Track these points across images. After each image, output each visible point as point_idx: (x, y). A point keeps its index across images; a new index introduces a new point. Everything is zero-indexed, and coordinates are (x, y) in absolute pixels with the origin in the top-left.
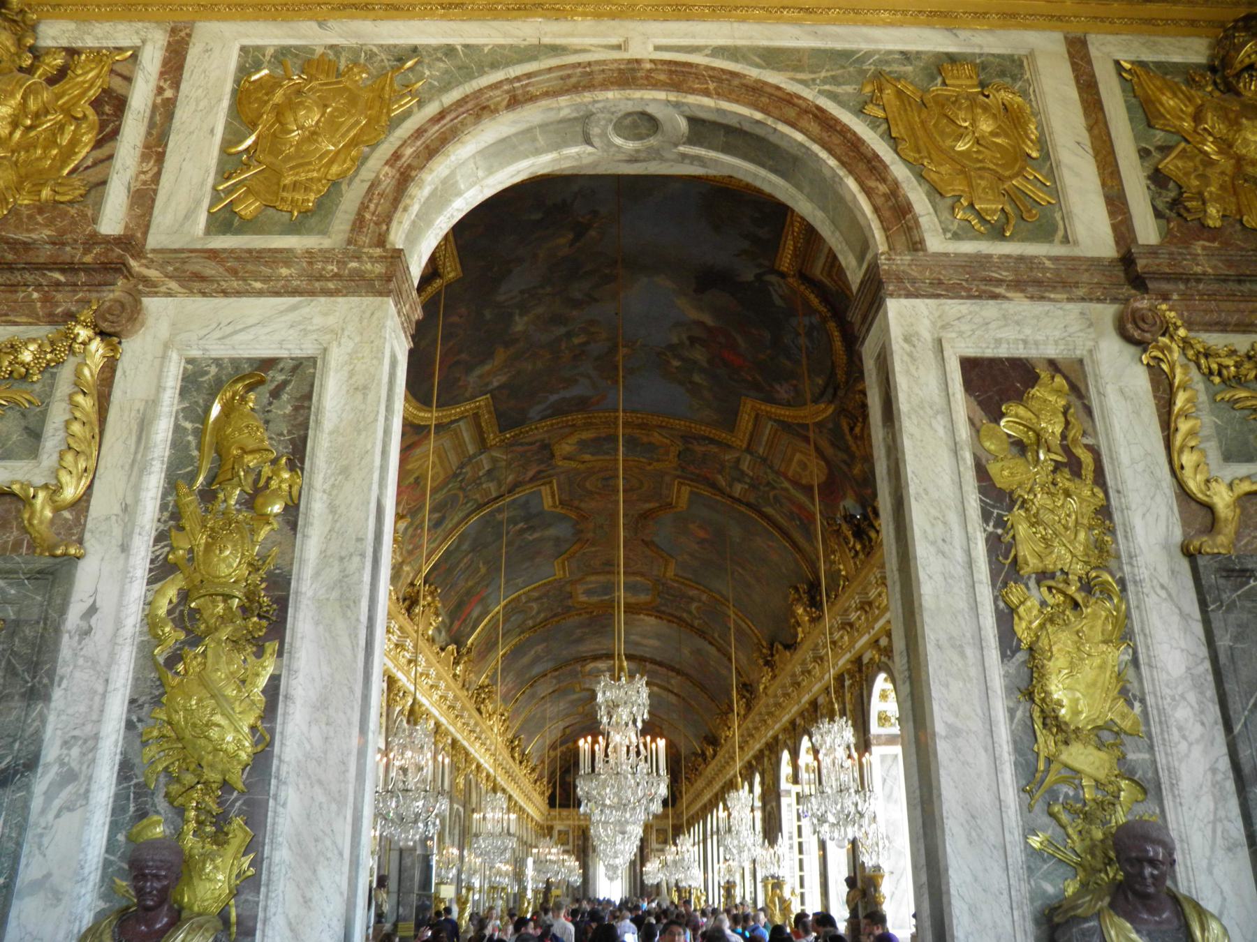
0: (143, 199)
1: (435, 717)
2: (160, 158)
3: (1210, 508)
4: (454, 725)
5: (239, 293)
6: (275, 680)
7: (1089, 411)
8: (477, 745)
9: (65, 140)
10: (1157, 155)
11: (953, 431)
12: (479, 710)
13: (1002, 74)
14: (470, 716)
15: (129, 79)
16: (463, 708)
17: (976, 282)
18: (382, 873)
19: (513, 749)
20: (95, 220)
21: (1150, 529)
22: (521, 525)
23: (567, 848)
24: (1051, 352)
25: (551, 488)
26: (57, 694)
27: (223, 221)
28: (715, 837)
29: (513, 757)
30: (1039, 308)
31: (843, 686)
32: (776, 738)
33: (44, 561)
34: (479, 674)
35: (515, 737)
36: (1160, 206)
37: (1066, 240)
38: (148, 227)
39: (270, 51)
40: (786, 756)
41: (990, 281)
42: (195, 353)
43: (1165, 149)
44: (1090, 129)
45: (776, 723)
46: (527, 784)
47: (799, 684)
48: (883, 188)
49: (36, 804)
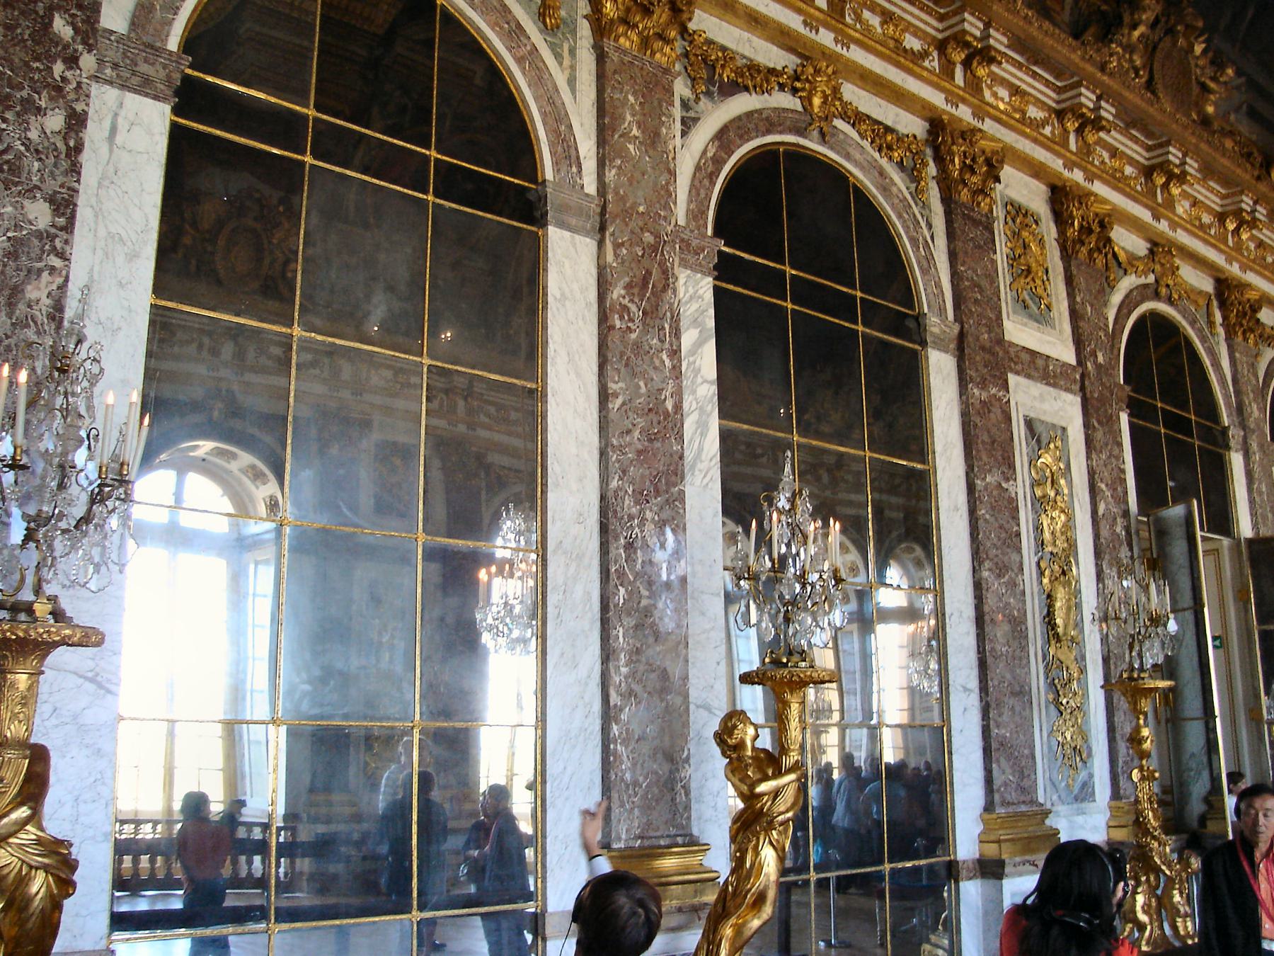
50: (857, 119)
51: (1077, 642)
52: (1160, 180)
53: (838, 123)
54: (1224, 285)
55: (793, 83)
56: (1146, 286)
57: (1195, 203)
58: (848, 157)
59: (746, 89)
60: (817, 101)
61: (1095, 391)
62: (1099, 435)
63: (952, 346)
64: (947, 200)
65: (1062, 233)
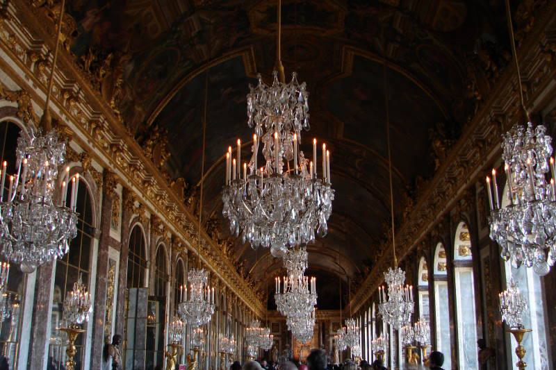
1: (171, 231)
4: (190, 241)
8: (210, 260)
12: (210, 236)
16: (196, 229)
18: (119, 333)
19: (239, 268)
22: (229, 89)
23: (277, 334)
25: (250, 54)
28: (370, 326)
31: (474, 195)
32: (415, 250)
35: (241, 260)
40: (422, 262)
45: (414, 239)
46: (250, 292)
47: (434, 205)
50: (92, 169)
51: (111, 324)
52: (146, 185)
53: (88, 171)
54: (153, 217)
55: (82, 157)
56: (136, 218)
57: (152, 191)
58: (87, 181)
59: (73, 160)
60: (86, 164)
61: (123, 251)
62: (123, 265)
63: (99, 237)
64: (104, 193)
65: (123, 202)
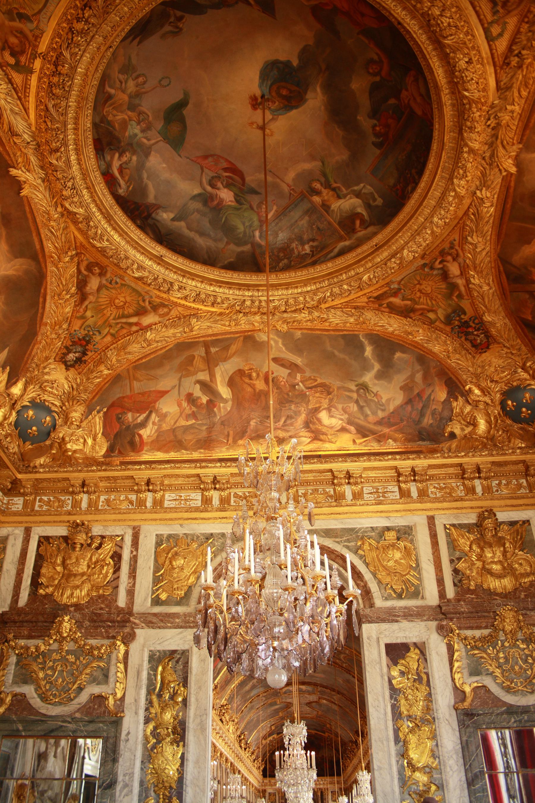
0: (131, 593)
2: (134, 577)
3: (464, 692)
5: (164, 628)
6: (183, 754)
7: (426, 660)
8: (220, 740)
9: (104, 572)
10: (456, 561)
11: (381, 669)
13: (405, 533)
14: (217, 725)
15: (121, 547)
17: (390, 616)
19: (240, 741)
20: (116, 601)
21: (444, 700)
24: (414, 640)
26: (121, 760)
27: (156, 601)
29: (241, 746)
30: (411, 624)
33: (114, 719)
34: (221, 698)
35: (241, 733)
36: (456, 582)
37: (423, 598)
38: (133, 603)
39: (165, 536)
41: (395, 616)
42: (152, 648)
43: (459, 559)
44: (433, 554)
46: (249, 763)
48: (362, 584)
49: (118, 794)
